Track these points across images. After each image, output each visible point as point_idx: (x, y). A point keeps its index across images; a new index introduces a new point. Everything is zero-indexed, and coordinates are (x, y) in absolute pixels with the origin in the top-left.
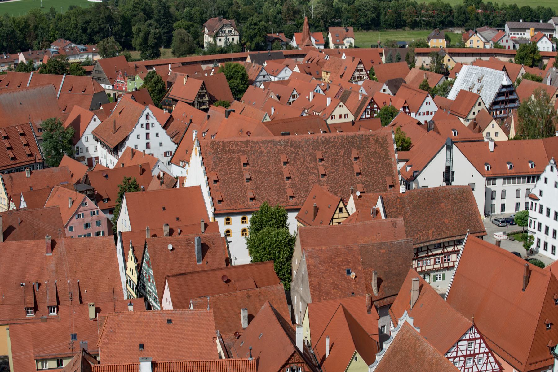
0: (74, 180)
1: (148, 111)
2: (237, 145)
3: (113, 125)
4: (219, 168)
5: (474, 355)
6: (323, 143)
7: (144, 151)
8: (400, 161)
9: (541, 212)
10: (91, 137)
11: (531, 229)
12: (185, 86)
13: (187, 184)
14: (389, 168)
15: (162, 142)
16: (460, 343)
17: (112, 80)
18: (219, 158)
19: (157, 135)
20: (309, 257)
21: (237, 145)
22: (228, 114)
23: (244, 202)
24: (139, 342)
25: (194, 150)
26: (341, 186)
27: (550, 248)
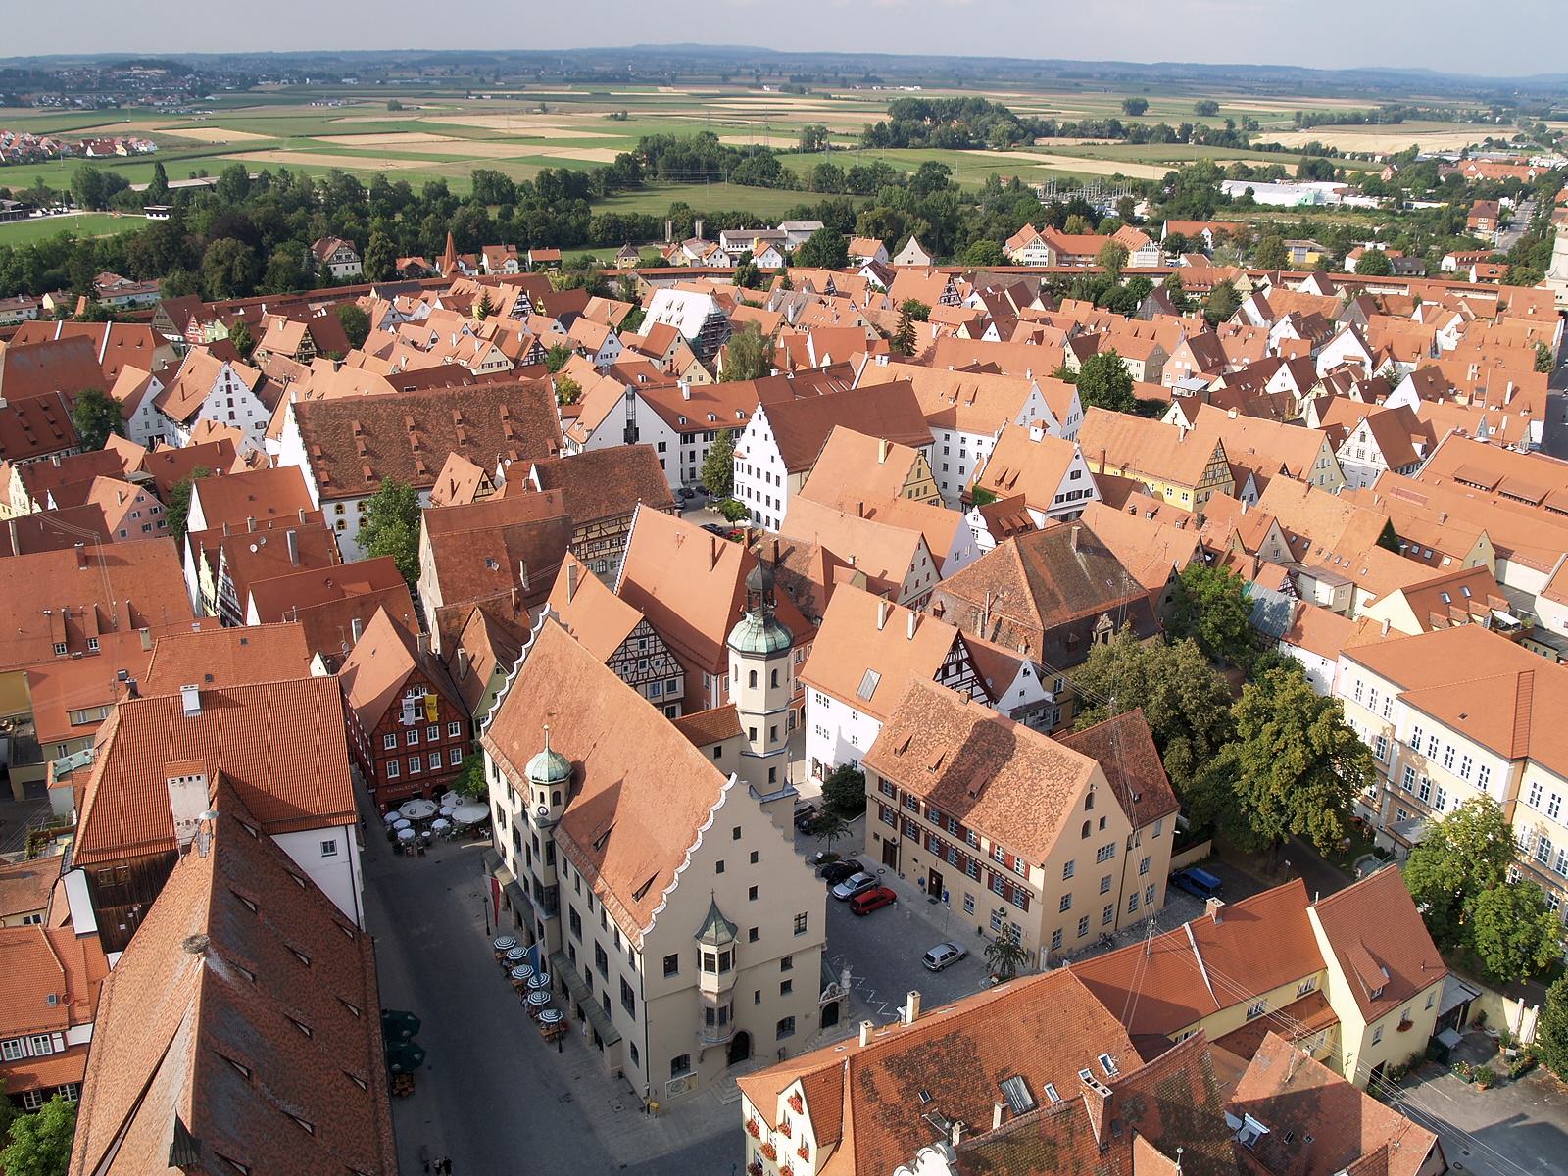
5: (649, 656)
6: (461, 399)
9: (749, 473)
11: (741, 498)
13: (279, 465)
16: (628, 642)
20: (434, 545)
21: (345, 408)
23: (359, 482)
24: (204, 673)
26: (487, 455)
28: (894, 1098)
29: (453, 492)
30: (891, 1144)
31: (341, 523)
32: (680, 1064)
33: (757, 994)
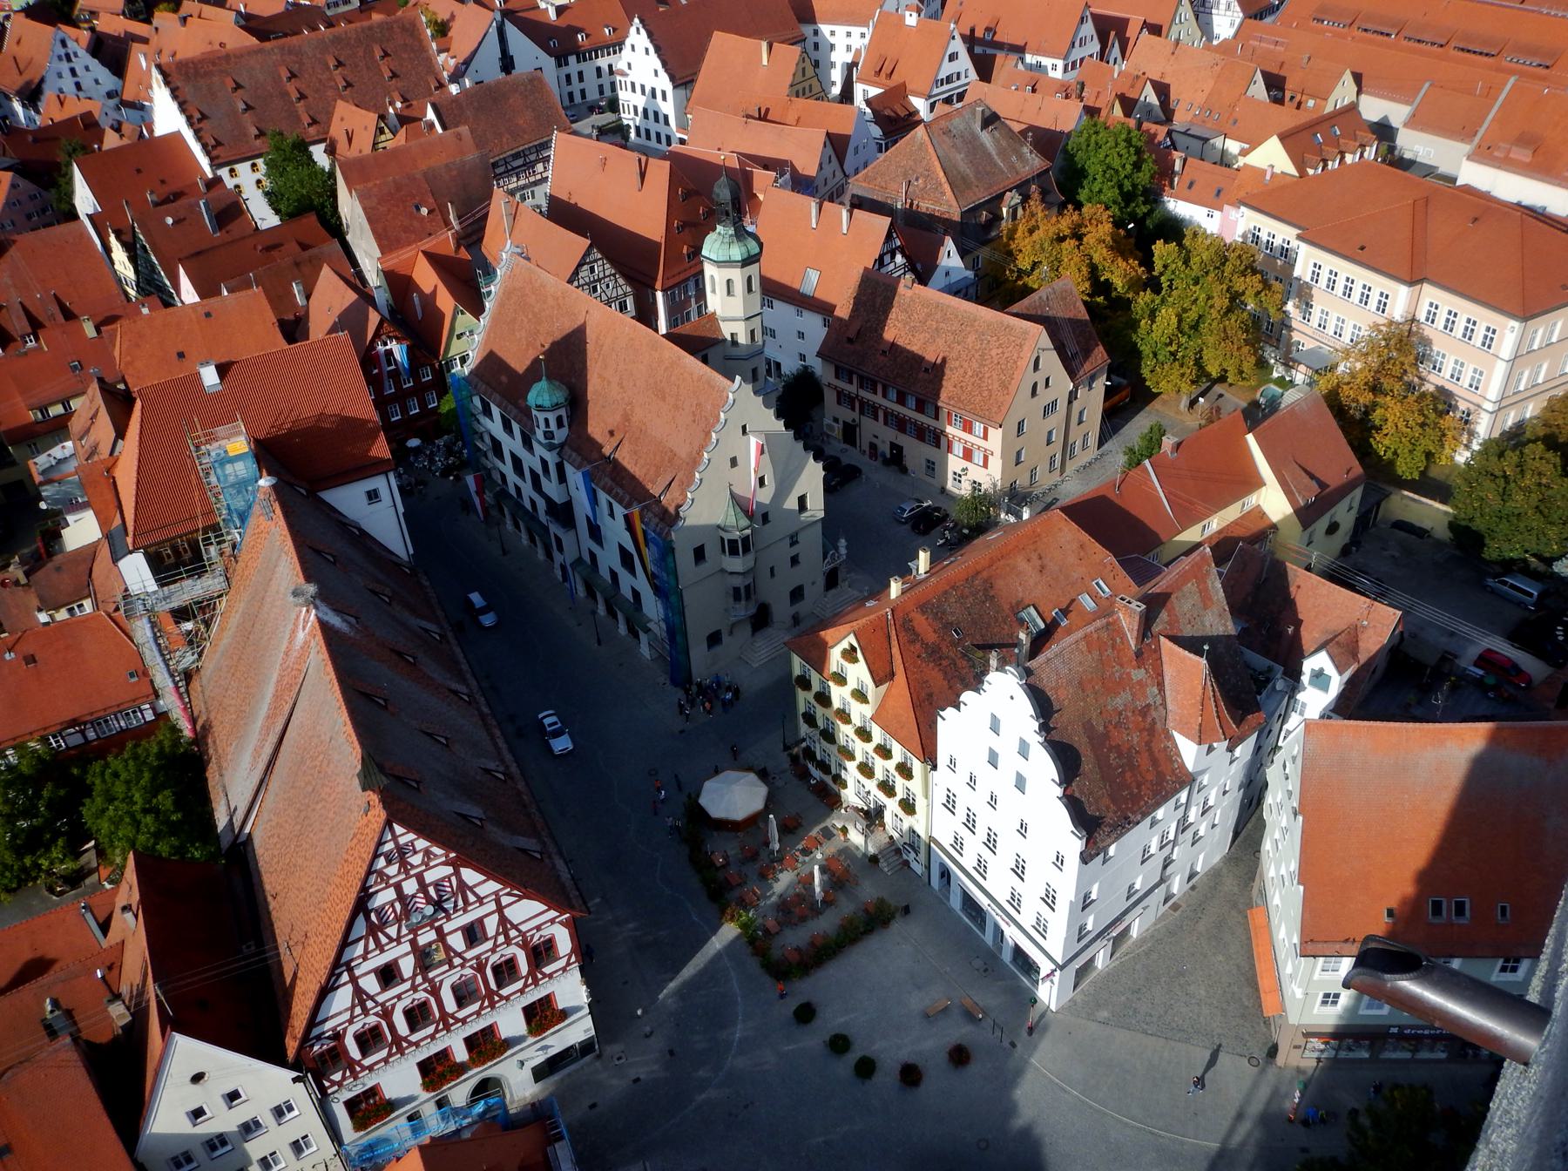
5: (599, 280)
6: (332, 42)
8: (440, 51)
9: (634, 90)
14: (429, 64)
20: (362, 199)
21: (214, 64)
27: (653, 136)
28: (931, 637)
29: (350, 140)
30: (935, 677)
31: (237, 186)
32: (714, 639)
33: (772, 569)
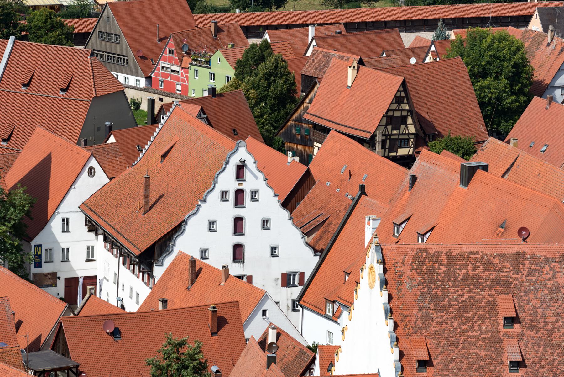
0: (23, 340)
1: (242, 154)
2: (488, 265)
3: (142, 191)
4: (434, 326)
7: (226, 267)
10: (78, 222)
12: (349, 91)
15: (278, 247)
17: (146, 63)
18: (436, 299)
19: (265, 224)
21: (488, 265)
22: (468, 175)
25: (366, 271)
